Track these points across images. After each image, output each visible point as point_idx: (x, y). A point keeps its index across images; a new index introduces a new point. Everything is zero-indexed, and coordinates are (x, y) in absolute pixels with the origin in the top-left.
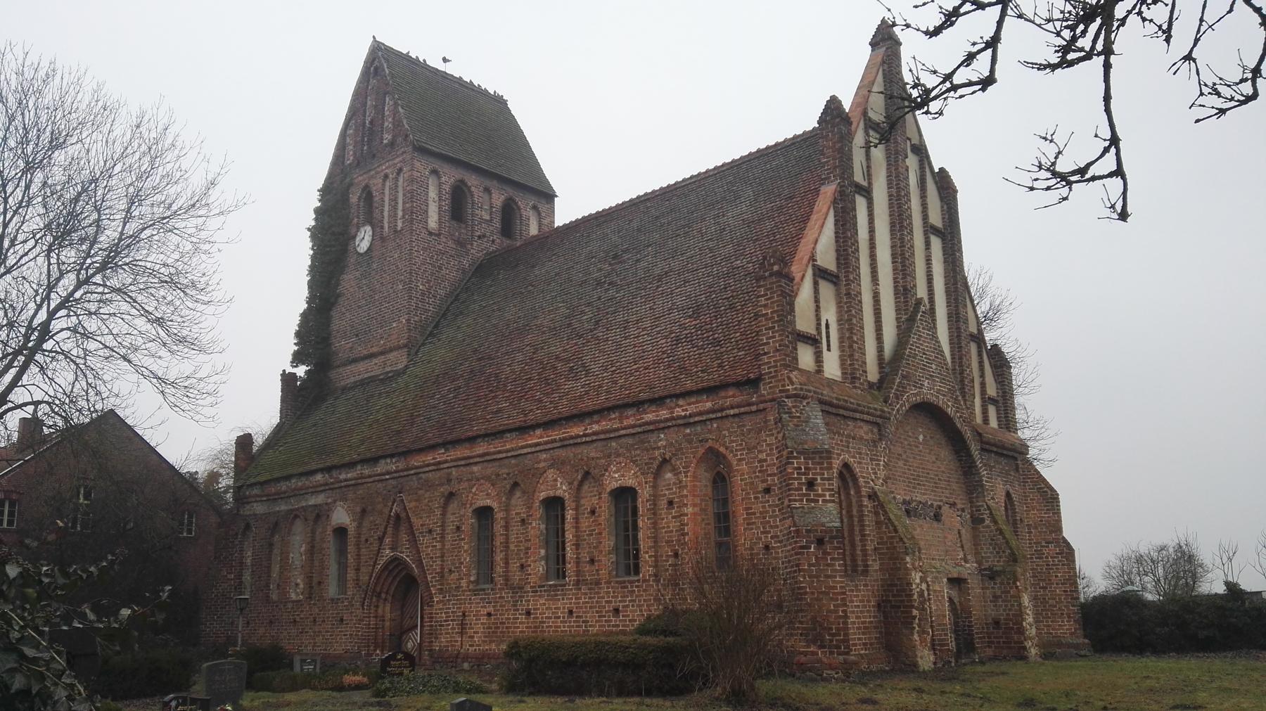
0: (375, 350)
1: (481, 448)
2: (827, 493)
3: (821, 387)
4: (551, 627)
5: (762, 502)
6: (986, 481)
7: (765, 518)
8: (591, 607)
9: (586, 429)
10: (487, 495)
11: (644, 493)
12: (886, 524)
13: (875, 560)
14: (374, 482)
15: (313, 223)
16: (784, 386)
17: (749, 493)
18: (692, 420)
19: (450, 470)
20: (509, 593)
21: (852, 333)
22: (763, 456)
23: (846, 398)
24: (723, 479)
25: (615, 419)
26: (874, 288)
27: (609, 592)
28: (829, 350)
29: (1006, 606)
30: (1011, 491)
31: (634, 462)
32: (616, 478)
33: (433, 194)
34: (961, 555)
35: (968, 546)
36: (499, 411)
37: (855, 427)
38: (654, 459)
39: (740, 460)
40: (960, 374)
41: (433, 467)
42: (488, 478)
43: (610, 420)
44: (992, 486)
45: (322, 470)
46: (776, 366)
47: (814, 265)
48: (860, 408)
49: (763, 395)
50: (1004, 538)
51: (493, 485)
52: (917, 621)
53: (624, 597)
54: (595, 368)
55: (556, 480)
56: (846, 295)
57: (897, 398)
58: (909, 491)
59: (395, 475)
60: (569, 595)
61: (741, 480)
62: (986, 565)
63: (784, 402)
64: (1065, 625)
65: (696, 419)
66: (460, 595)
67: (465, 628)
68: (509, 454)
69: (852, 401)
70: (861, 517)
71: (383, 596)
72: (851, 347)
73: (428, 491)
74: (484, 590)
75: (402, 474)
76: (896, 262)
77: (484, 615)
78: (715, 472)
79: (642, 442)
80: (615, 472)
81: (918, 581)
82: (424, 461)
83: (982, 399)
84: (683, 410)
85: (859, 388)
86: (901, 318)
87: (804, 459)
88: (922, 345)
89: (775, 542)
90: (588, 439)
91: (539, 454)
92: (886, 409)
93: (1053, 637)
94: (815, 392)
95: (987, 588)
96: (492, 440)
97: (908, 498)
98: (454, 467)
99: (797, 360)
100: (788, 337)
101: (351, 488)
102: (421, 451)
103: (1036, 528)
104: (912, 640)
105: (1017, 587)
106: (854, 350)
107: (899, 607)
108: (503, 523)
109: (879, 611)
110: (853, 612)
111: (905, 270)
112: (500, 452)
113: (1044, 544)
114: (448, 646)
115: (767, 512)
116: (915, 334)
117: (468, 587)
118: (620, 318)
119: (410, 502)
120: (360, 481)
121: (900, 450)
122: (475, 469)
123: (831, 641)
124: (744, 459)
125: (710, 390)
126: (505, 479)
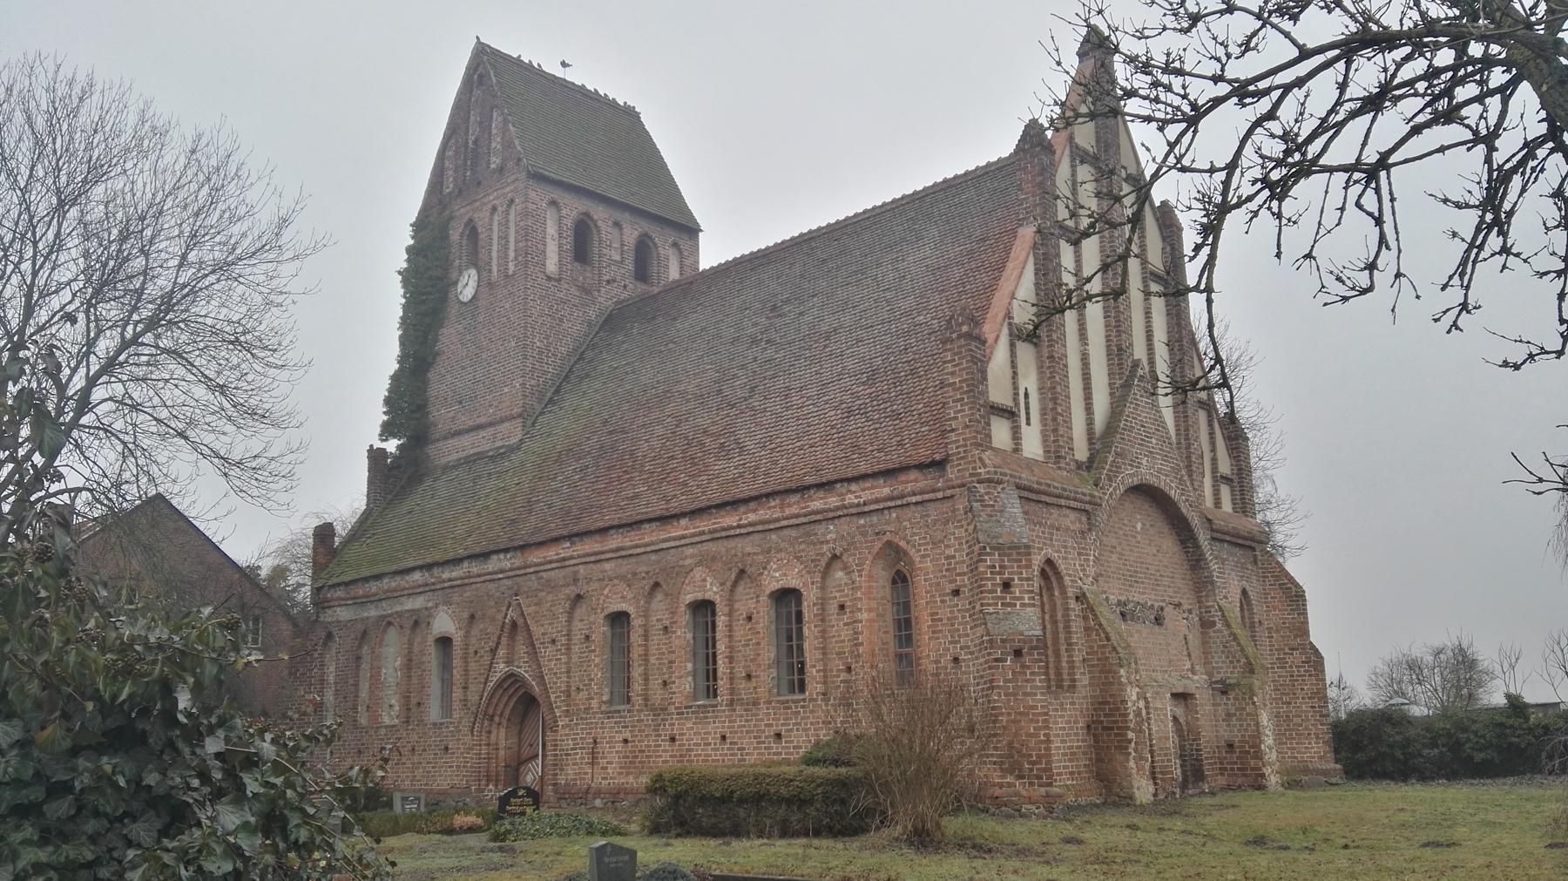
0: (483, 420)
1: (615, 541)
2: (1026, 596)
3: (1020, 470)
4: (700, 755)
5: (949, 606)
6: (1218, 577)
7: (953, 625)
8: (747, 732)
9: (741, 519)
10: (622, 597)
11: (810, 596)
12: (1097, 630)
13: (1084, 674)
15: (405, 265)
16: (974, 468)
18: (866, 509)
19: (576, 568)
21: (1055, 403)
22: (950, 552)
23: (1049, 482)
24: (904, 580)
25: (775, 507)
26: (1082, 348)
28: (1028, 424)
29: (1241, 725)
30: (1248, 588)
31: (798, 558)
32: (776, 579)
33: (551, 230)
34: (1188, 666)
35: (1196, 653)
36: (636, 496)
37: (1059, 515)
38: (823, 555)
39: (924, 556)
40: (1186, 448)
41: (557, 565)
42: (622, 578)
43: (769, 508)
44: (1224, 583)
45: (421, 568)
46: (966, 445)
47: (1010, 324)
48: (1066, 494)
49: (951, 480)
50: (1239, 644)
51: (629, 586)
52: (1133, 745)
53: (787, 719)
54: (750, 445)
55: (704, 580)
56: (1048, 358)
57: (1110, 479)
58: (1125, 590)
60: (721, 717)
61: (925, 580)
62: (1217, 677)
63: (975, 487)
64: (1313, 748)
66: (590, 718)
67: (597, 758)
68: (649, 549)
69: (1056, 484)
70: (1067, 621)
71: (497, 719)
72: (1054, 420)
73: (549, 593)
74: (619, 712)
75: (518, 572)
76: (1109, 316)
77: (619, 742)
79: (808, 534)
80: (775, 571)
81: (1134, 697)
82: (544, 557)
83: (1213, 477)
85: (1065, 469)
86: (1115, 384)
87: (999, 555)
88: (1140, 416)
91: (684, 548)
92: (1097, 494)
93: (1298, 762)
94: (1011, 476)
95: (1220, 705)
96: (628, 532)
97: (1123, 598)
98: (582, 563)
99: (990, 437)
100: (979, 410)
101: (456, 589)
102: (541, 544)
103: (1277, 631)
104: (1127, 768)
105: (1254, 703)
106: (1059, 424)
107: (1112, 729)
108: (641, 631)
109: (1088, 734)
110: (1058, 735)
111: (1119, 326)
112: (637, 546)
113: (1287, 650)
114: (576, 780)
115: (956, 618)
116: (1132, 403)
117: (600, 708)
118: (780, 384)
119: (529, 606)
120: (466, 581)
121: (1114, 542)
122: (607, 566)
123: (1031, 770)
124: (928, 555)
126: (644, 578)
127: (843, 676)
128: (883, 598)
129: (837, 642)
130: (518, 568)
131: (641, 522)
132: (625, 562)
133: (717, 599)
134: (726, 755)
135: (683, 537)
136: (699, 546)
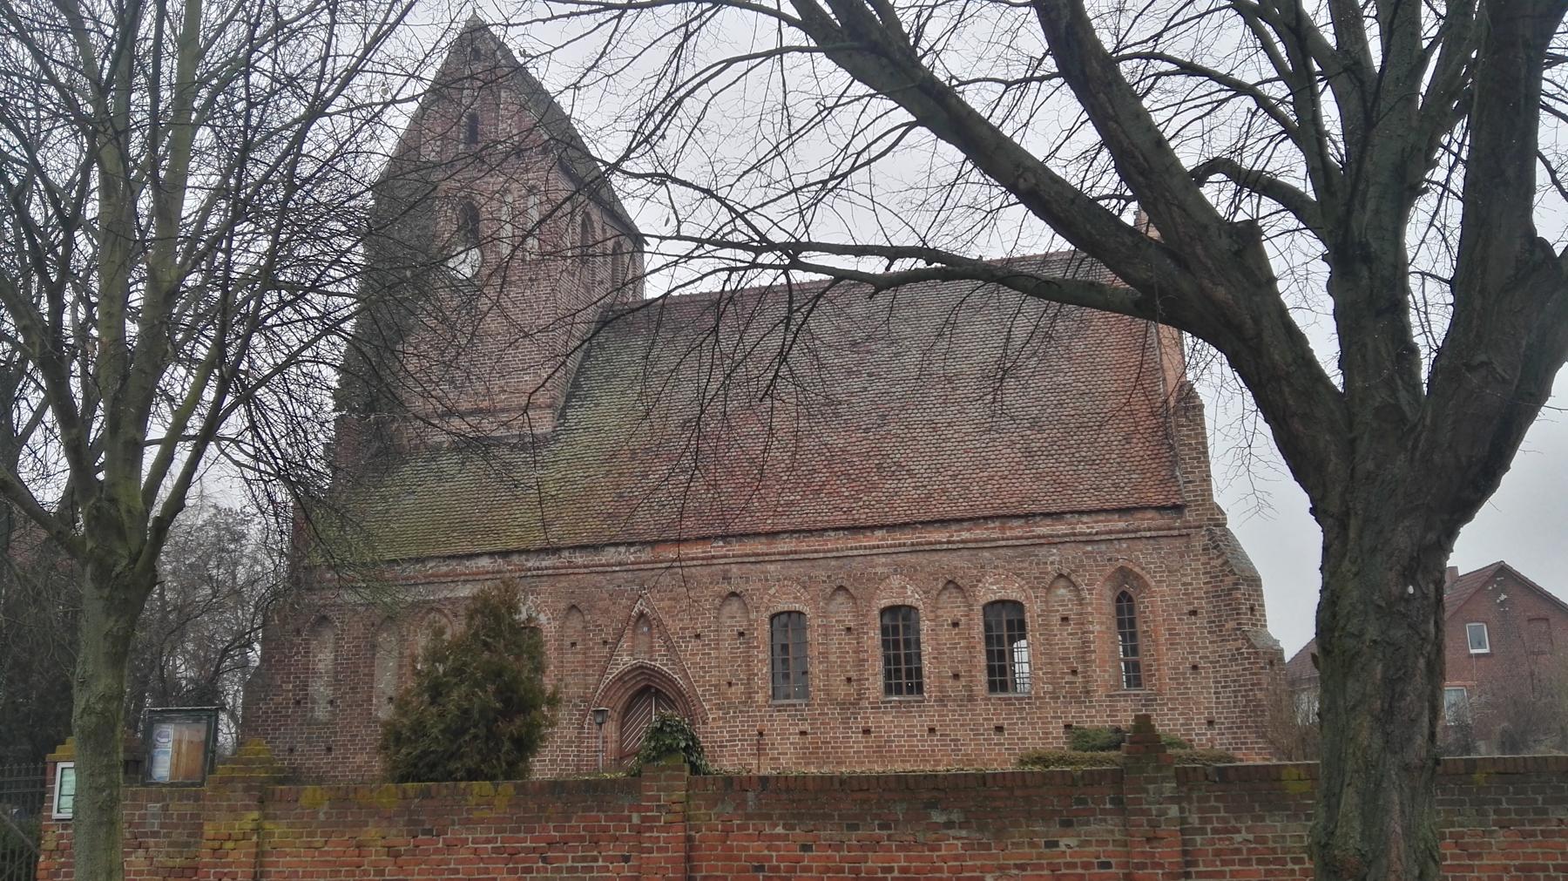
1: (785, 545)
7: (1191, 639)
8: (961, 725)
9: (952, 536)
10: (795, 598)
14: (591, 573)
17: (1172, 615)
18: (1096, 538)
19: (727, 567)
20: (835, 709)
22: (1188, 579)
25: (994, 528)
27: (989, 710)
32: (991, 590)
38: (1047, 573)
39: (1160, 581)
41: (700, 562)
43: (986, 529)
45: (491, 554)
46: (1204, 495)
53: (1010, 714)
55: (905, 587)
59: (631, 567)
60: (929, 711)
65: (1103, 537)
74: (794, 705)
75: (642, 566)
78: (1119, 591)
80: (991, 584)
84: (1088, 528)
89: (1205, 663)
90: (950, 546)
91: (875, 557)
96: (804, 537)
98: (737, 563)
101: (545, 579)
112: (816, 551)
122: (771, 567)
124: (1165, 581)
125: (1122, 511)
127: (1068, 678)
128: (1109, 614)
129: (1060, 649)
130: (644, 563)
131: (825, 530)
132: (796, 565)
133: (920, 605)
134: (937, 746)
135: (878, 547)
136: (894, 556)
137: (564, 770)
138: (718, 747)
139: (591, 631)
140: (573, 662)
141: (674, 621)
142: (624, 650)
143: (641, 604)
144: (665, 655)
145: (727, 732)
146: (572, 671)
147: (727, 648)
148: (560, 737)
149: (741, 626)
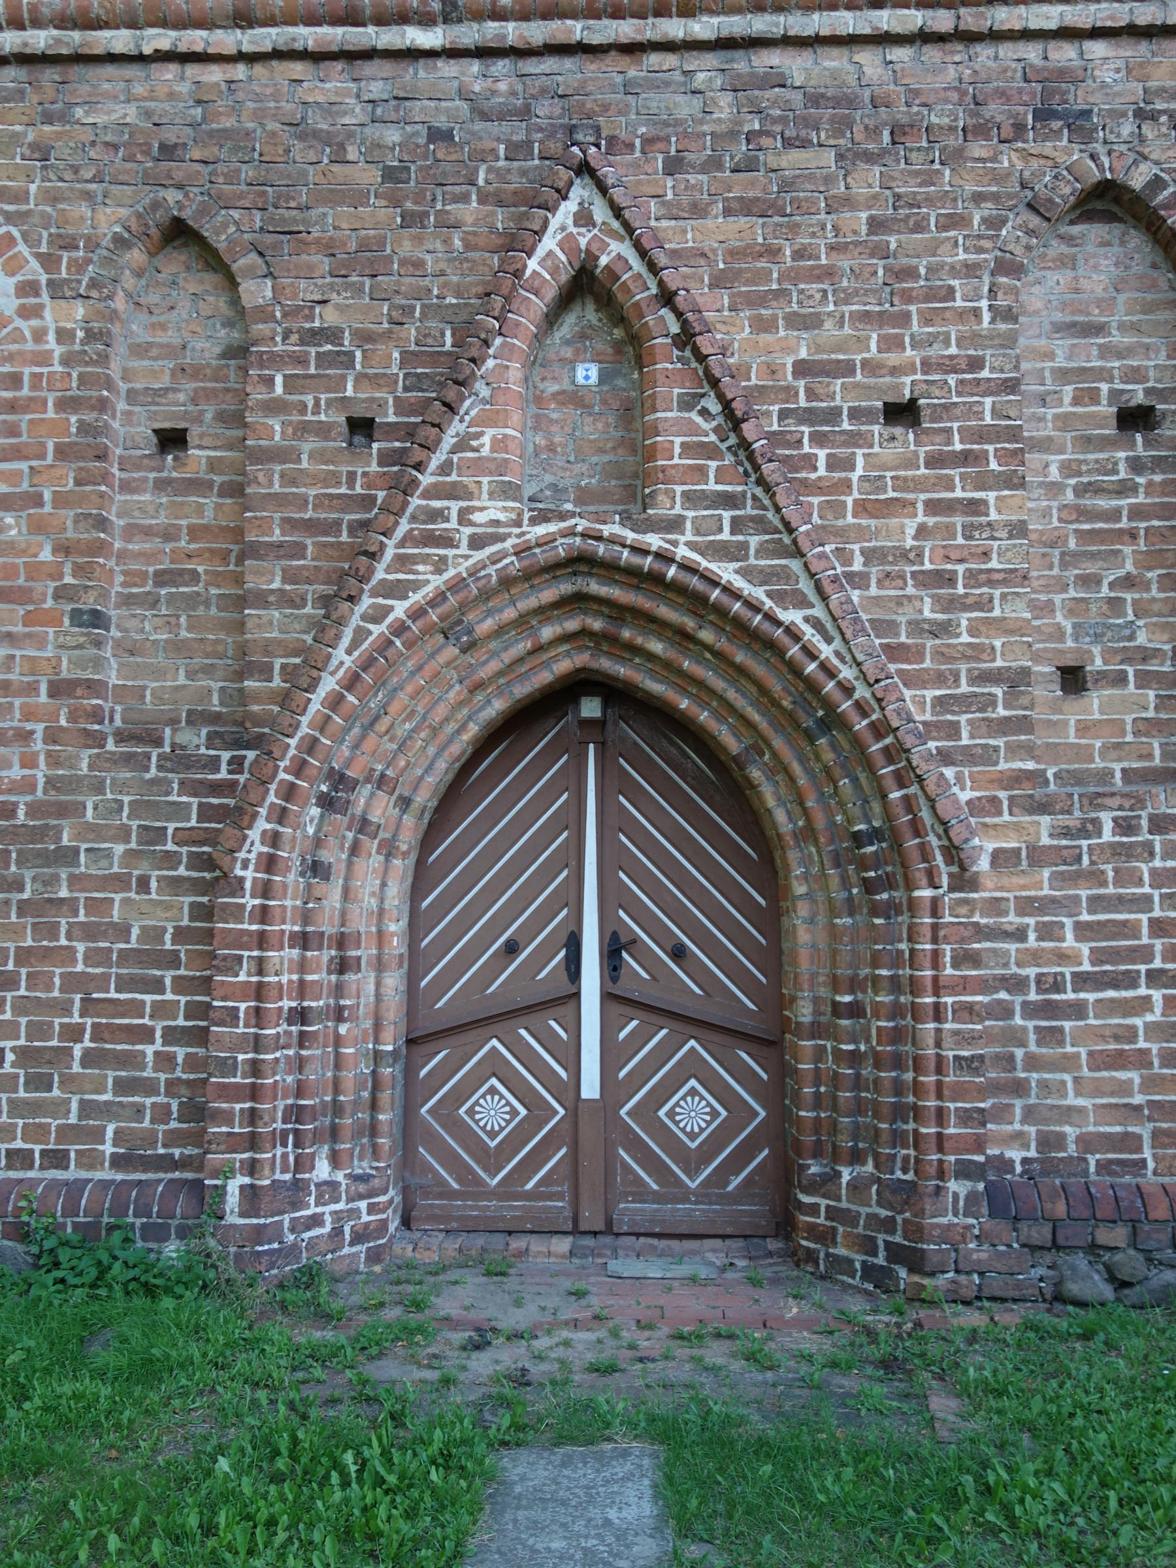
19: (1065, 54)
137: (107, 1111)
138: (1031, 1011)
139: (276, 360)
140: (169, 535)
141: (763, 326)
142: (479, 467)
143: (584, 218)
144: (730, 501)
145: (1083, 931)
146: (162, 578)
147: (1054, 489)
148: (89, 932)
149: (1135, 376)
